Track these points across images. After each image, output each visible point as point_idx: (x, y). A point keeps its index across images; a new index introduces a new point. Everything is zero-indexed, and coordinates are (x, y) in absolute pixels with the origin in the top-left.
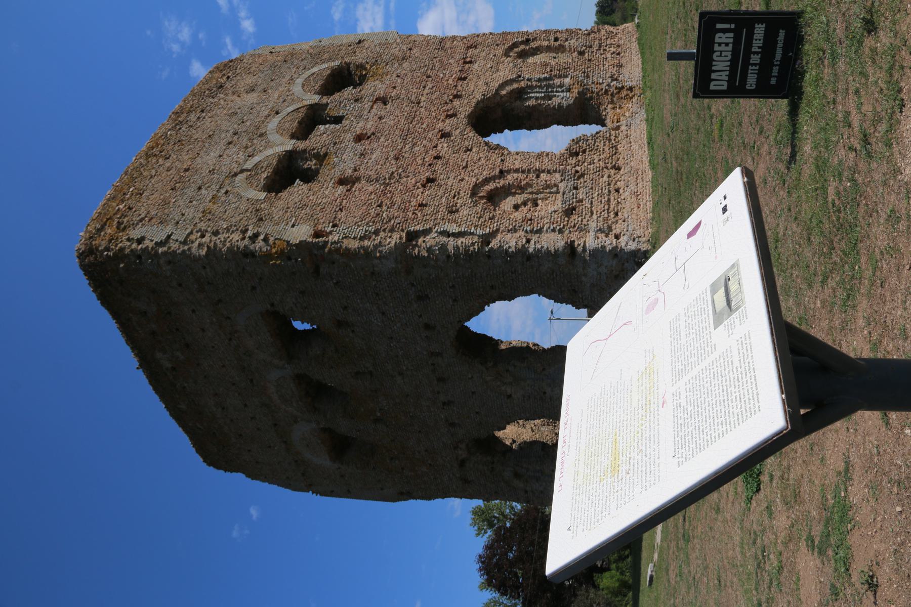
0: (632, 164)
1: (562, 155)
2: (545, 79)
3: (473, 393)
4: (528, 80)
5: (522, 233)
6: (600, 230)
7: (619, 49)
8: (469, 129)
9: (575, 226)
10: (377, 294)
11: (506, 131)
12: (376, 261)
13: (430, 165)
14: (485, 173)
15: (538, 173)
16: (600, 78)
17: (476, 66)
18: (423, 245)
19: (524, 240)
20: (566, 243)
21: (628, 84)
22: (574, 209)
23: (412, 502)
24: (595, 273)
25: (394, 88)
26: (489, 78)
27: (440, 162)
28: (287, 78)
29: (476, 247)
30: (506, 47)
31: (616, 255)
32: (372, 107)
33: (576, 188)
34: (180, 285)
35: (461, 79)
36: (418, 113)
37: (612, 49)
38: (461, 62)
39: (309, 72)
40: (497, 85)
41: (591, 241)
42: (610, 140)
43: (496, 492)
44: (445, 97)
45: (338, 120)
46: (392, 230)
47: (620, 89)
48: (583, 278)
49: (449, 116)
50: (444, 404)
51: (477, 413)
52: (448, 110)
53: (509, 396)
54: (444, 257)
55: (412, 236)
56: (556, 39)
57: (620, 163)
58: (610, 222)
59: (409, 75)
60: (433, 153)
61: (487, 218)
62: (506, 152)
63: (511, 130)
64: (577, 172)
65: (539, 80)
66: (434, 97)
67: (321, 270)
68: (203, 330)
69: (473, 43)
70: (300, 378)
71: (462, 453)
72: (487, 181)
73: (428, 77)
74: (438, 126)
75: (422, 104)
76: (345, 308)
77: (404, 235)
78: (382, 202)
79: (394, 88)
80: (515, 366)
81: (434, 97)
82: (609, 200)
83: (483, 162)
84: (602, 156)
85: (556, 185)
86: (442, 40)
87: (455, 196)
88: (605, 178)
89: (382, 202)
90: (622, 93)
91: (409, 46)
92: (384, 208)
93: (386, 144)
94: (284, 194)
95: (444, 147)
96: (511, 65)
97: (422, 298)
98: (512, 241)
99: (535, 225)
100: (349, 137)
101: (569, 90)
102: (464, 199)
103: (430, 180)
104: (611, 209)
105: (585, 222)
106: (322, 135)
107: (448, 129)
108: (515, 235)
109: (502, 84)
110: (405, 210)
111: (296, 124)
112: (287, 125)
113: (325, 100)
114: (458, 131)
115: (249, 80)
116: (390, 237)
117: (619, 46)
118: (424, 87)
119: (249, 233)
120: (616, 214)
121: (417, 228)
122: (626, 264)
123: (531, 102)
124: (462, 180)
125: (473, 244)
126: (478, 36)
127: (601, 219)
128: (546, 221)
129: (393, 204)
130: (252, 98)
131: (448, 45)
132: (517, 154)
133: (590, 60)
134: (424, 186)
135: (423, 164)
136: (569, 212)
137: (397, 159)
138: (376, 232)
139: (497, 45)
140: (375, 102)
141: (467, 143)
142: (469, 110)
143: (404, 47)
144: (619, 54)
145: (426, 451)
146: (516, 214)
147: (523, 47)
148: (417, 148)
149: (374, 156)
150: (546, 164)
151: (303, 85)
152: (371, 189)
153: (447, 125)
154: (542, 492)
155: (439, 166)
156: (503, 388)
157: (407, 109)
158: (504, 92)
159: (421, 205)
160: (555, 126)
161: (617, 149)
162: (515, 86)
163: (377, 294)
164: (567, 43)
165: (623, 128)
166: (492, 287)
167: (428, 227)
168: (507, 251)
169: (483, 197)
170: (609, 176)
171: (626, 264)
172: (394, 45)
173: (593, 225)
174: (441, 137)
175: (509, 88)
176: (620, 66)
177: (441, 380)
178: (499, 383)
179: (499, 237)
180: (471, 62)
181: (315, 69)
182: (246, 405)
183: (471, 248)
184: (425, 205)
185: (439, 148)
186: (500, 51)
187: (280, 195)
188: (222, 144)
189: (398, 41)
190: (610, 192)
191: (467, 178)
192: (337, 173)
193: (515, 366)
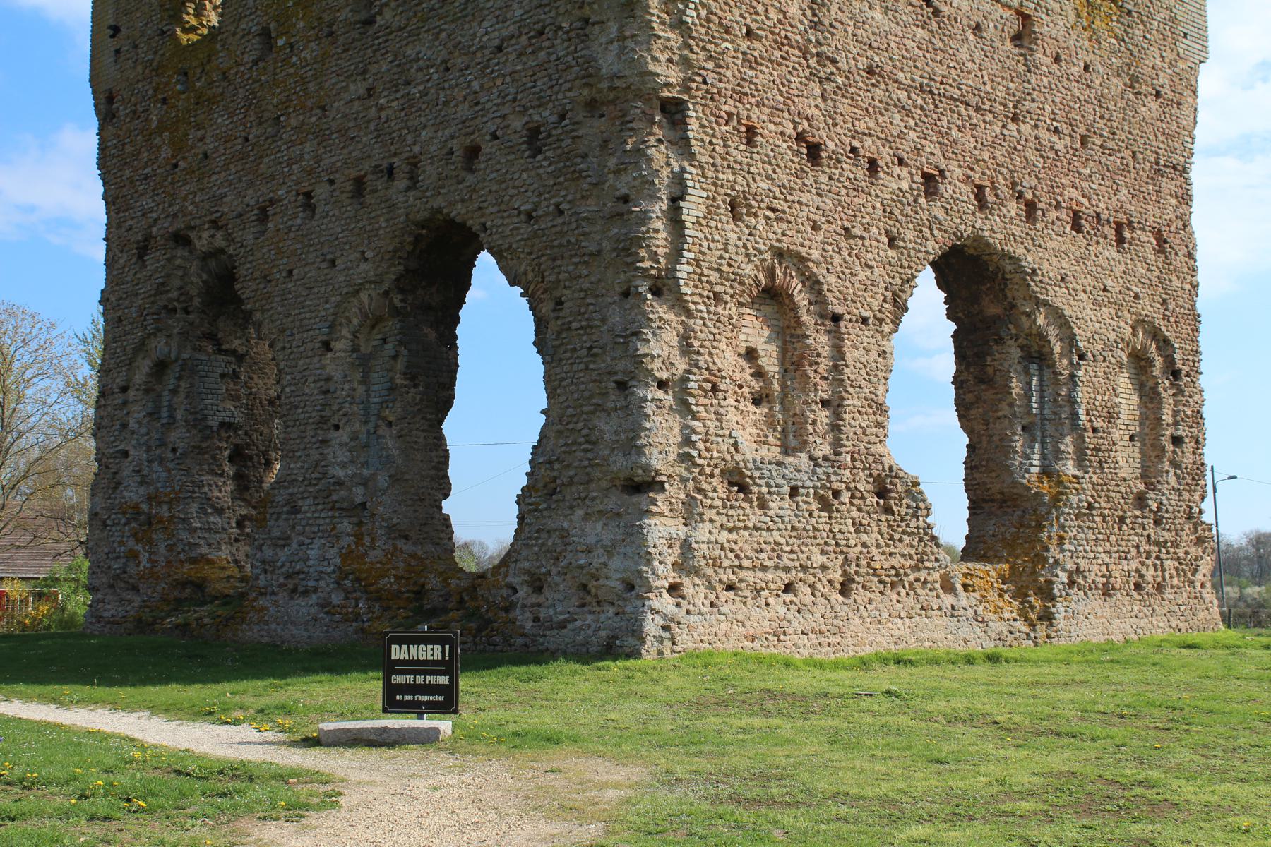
0: (857, 621)
1: (879, 459)
2: (1074, 416)
3: (333, 263)
4: (1072, 376)
5: (681, 366)
6: (686, 546)
7: (1150, 589)
9: (699, 490)
10: (541, 33)
11: (952, 327)
12: (613, 29)
13: (854, 150)
14: (832, 279)
15: (834, 405)
16: (1075, 548)
17: (1111, 252)
18: (652, 140)
19: (664, 375)
20: (657, 471)
21: (1060, 610)
22: (743, 489)
23: (93, 124)
24: (592, 540)
25: (1057, 59)
26: (1079, 288)
27: (860, 173)
29: (647, 264)
30: (1159, 322)
31: (631, 587)
33: (794, 492)
36: (989, 117)
37: (1149, 574)
38: (1122, 217)
40: (1058, 303)
41: (662, 529)
42: (916, 568)
43: (120, 320)
46: (686, 62)
47: (1047, 593)
48: (580, 513)
49: (979, 191)
50: (308, 195)
51: (290, 272)
52: (994, 188)
53: (327, 346)
54: (625, 191)
55: (674, 112)
56: (1177, 441)
57: (860, 595)
58: (710, 572)
60: (885, 156)
61: (719, 288)
62: (886, 328)
63: (955, 336)
64: (836, 494)
65: (1072, 401)
66: (1032, 155)
69: (1173, 246)
71: (203, 240)
72: (813, 284)
73: (1084, 140)
74: (953, 166)
75: (1012, 126)
77: (674, 94)
78: (758, 38)
79: (1057, 59)
80: (395, 357)
81: (1032, 155)
82: (764, 568)
83: (862, 276)
84: (874, 550)
85: (803, 445)
86: (1182, 171)
87: (773, 210)
88: (818, 559)
89: (758, 38)
90: (1034, 592)
91: (1166, 91)
92: (744, 45)
93: (909, 43)
95: (900, 181)
96: (1112, 336)
98: (661, 348)
99: (703, 400)
101: (1046, 472)
102: (767, 234)
103: (814, 152)
104: (742, 574)
105: (709, 513)
107: (946, 190)
108: (676, 352)
109: (1062, 316)
110: (740, 96)
114: (940, 214)
116: (670, 60)
117: (1159, 588)
118: (1056, 131)
120: (730, 588)
121: (693, 125)
122: (612, 610)
123: (1016, 386)
124: (816, 227)
125: (654, 257)
126: (1190, 256)
127: (718, 552)
128: (712, 425)
132: (882, 354)
133: (1122, 520)
134: (800, 137)
135: (855, 134)
136: (738, 481)
137: (870, 71)
138: (679, 25)
139: (1164, 302)
140: (1019, 13)
141: (909, 235)
142: (996, 240)
143: (1163, 79)
144: (1138, 587)
145: (206, 156)
146: (730, 355)
147: (1163, 365)
148: (897, 117)
149: (878, 15)
150: (854, 422)
153: (955, 187)
154: (124, 426)
156: (345, 332)
157: (1001, 92)
158: (1041, 320)
159: (751, 132)
160: (966, 440)
161: (893, 585)
162: (1057, 349)
163: (541, 33)
164: (1166, 466)
165: (948, 600)
166: (559, 302)
167: (695, 149)
168: (637, 334)
169: (771, 273)
170: (824, 568)
171: (612, 610)
172: (1169, 55)
173: (702, 533)
174: (926, 176)
175: (1052, 333)
176: (1107, 591)
177: (359, 185)
178: (355, 321)
179: (671, 316)
180: (1120, 240)
183: (643, 253)
184: (750, 142)
185: (897, 170)
186: (1148, 307)
189: (1181, 65)
190: (787, 570)
191: (820, 237)
193: (395, 357)
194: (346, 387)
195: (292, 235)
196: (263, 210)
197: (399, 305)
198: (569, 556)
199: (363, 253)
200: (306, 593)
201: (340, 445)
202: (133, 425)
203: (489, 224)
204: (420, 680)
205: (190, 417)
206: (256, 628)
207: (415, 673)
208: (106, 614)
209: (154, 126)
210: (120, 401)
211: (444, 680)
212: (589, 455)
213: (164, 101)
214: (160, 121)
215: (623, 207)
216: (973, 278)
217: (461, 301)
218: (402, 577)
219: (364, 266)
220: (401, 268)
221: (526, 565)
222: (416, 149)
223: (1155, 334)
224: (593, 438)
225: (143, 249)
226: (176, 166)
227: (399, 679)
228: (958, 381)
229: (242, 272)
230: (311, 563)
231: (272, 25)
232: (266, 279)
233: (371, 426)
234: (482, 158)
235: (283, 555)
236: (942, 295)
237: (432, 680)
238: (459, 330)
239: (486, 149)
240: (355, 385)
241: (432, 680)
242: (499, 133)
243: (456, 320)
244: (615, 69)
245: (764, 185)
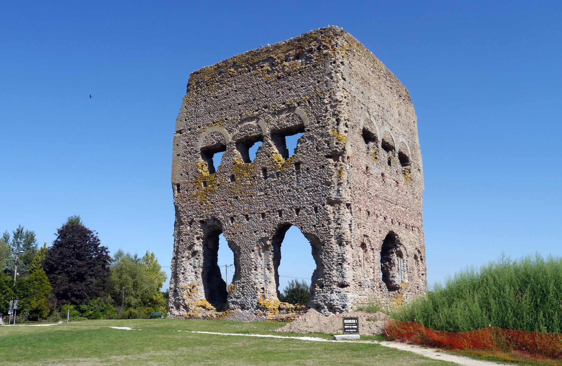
8: (388, 231)
17: (411, 233)
28: (405, 133)
38: (413, 225)
39: (407, 144)
44: (399, 218)
45: (389, 163)
59: (407, 199)
60: (378, 213)
68: (290, 90)
83: (377, 240)
94: (362, 139)
100: (383, 170)
106: (384, 155)
111: (387, 141)
112: (387, 136)
113: (397, 155)
115: (403, 112)
119: (348, 123)
129: (360, 196)
130: (397, 116)
131: (419, 218)
141: (383, 231)
147: (418, 257)
148: (380, 205)
151: (402, 142)
152: (365, 184)
155: (374, 217)
181: (408, 148)
182: (239, 104)
185: (381, 217)
186: (417, 245)
188: (379, 102)
192: (370, 166)
211: (356, 327)
215: (339, 226)
217: (282, 241)
223: (419, 251)
227: (346, 327)
237: (354, 327)
241: (354, 327)
243: (281, 246)
245: (362, 221)
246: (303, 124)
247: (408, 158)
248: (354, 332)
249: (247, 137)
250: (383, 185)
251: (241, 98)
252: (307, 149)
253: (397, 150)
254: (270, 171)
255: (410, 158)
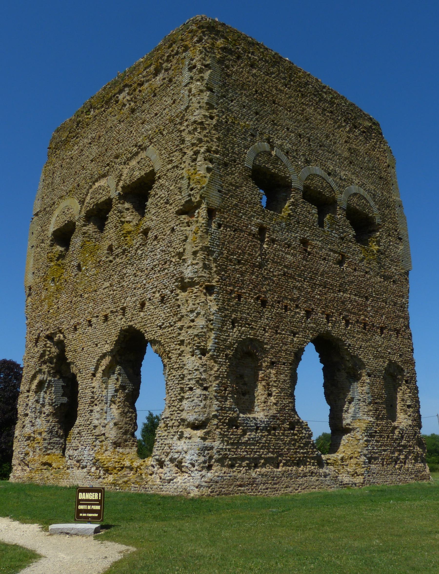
3: (97, 345)
32: (335, 252)
34: (174, 102)
35: (365, 325)
50: (90, 321)
63: (324, 369)
67: (183, 216)
70: (108, 204)
76: (156, 237)
94: (251, 184)
97: (163, 300)
103: (264, 303)
148: (296, 292)
154: (27, 405)
171: (187, 475)
174: (306, 311)
177: (106, 318)
182: (92, 161)
187: (250, 179)
193: (117, 379)
194: (100, 390)
195: (84, 335)
196: (75, 327)
197: (119, 360)
198: (172, 454)
199: (106, 341)
200: (83, 468)
201: (97, 412)
202: (30, 404)
203: (147, 330)
204: (89, 507)
205: (50, 401)
206: (65, 481)
207: (87, 504)
208: (17, 475)
209: (43, 298)
210: (26, 395)
212: (179, 415)
213: (47, 289)
214: (45, 296)
215: (192, 324)
216: (328, 348)
218: (116, 462)
219: (107, 346)
220: (119, 347)
221: (157, 457)
222: (125, 305)
224: (180, 409)
225: (37, 341)
226: (49, 312)
227: (81, 507)
228: (325, 386)
229: (67, 349)
230: (85, 456)
231: (82, 263)
232: (75, 351)
233: (108, 404)
234: (146, 307)
235: (76, 453)
236: (318, 354)
238: (142, 369)
239: (147, 304)
240: (103, 389)
242: (152, 298)
244: (190, 275)
246: (153, 170)
247: (373, 218)
248: (93, 518)
249: (97, 204)
250: (304, 259)
251: (95, 150)
252: (157, 205)
253: (344, 206)
254: (116, 249)
255: (378, 220)
